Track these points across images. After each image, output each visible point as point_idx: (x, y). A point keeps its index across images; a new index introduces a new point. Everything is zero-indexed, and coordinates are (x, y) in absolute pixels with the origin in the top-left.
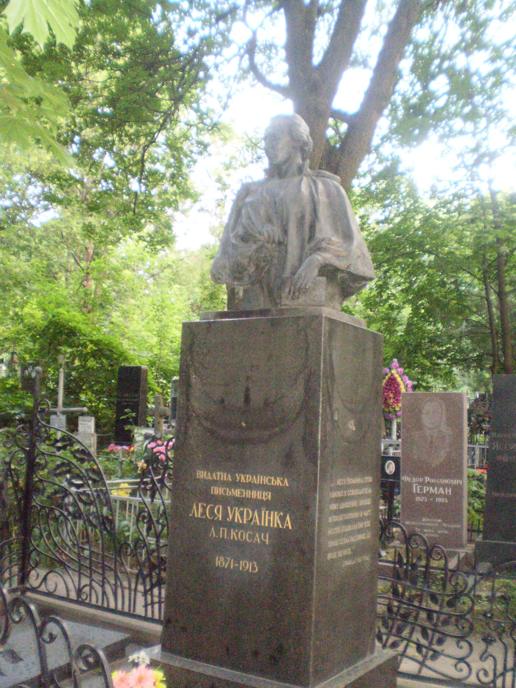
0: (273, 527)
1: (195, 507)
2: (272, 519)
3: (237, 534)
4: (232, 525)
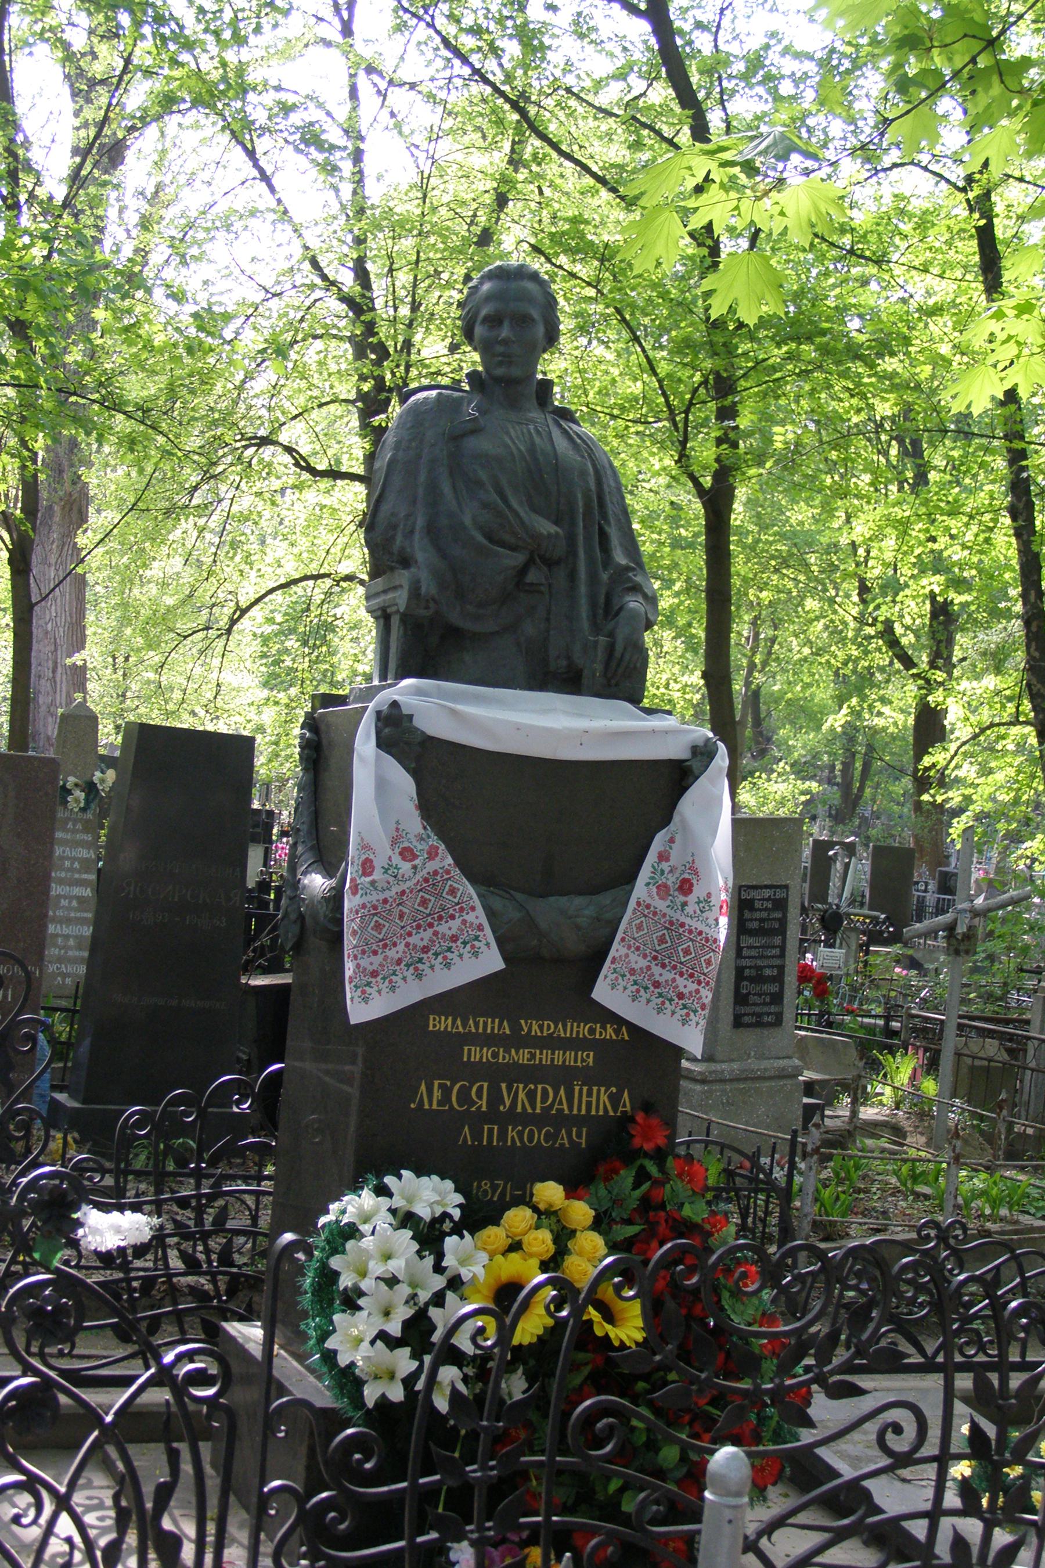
0: (597, 1117)
1: (423, 1087)
2: (599, 1101)
3: (520, 1134)
4: (513, 1117)
